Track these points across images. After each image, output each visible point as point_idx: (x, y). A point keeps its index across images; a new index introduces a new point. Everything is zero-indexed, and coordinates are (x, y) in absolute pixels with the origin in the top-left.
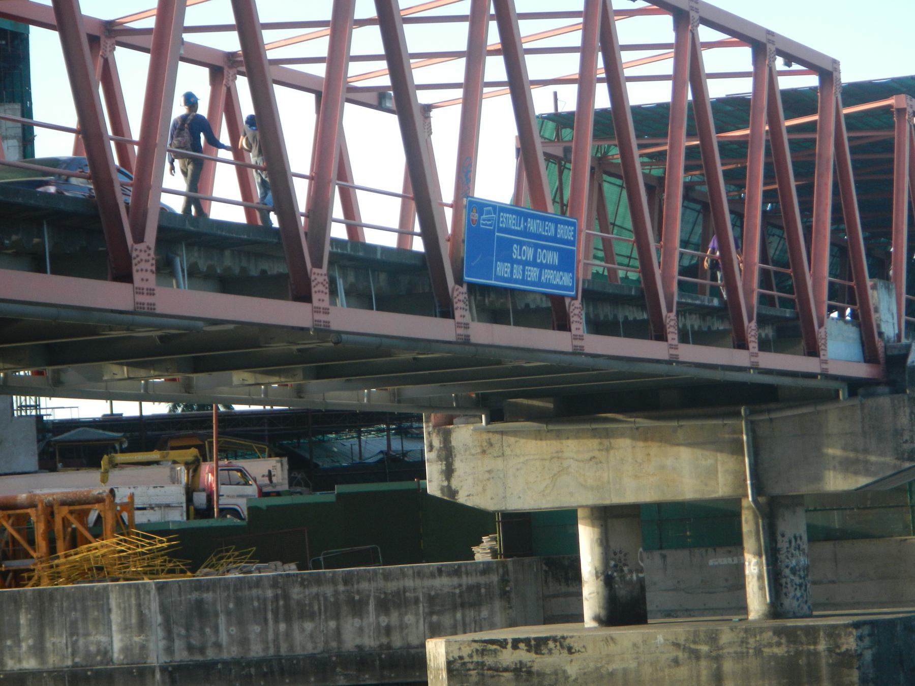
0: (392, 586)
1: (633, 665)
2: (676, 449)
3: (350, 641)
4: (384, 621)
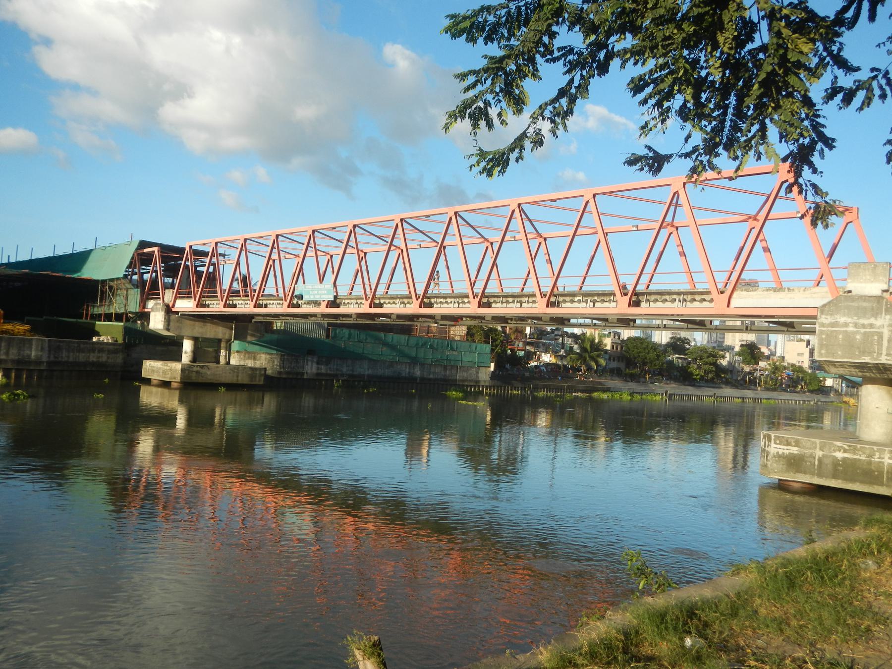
0: (101, 347)
1: (221, 372)
4: (99, 355)
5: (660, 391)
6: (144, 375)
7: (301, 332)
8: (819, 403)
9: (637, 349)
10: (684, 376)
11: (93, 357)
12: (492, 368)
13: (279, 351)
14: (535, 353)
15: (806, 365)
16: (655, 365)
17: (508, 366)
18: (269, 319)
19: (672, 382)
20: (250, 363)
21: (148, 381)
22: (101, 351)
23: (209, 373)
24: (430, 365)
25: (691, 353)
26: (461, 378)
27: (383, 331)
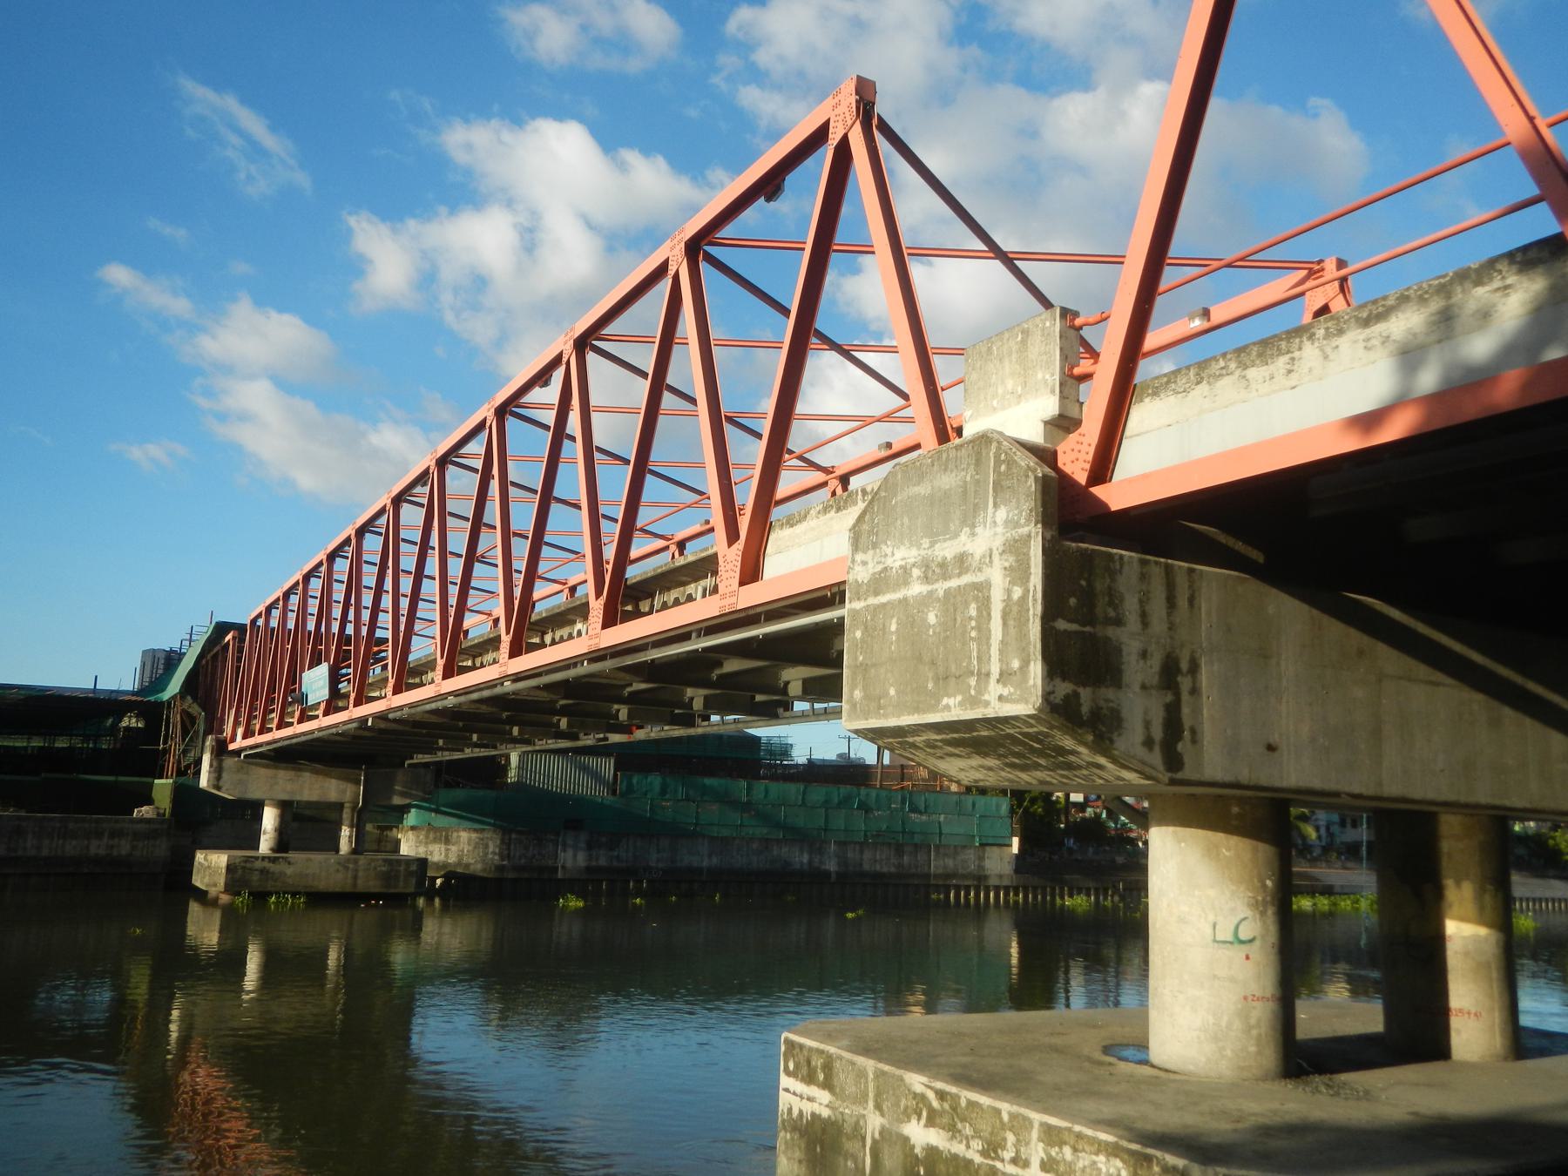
2: (328, 780)
3: (93, 850)
11: (97, 848)
12: (1015, 849)
24: (861, 844)
26: (940, 871)
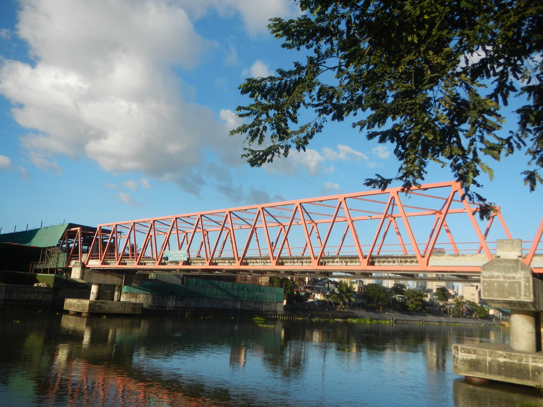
5: (390, 318)
6: (65, 308)
7: (166, 280)
8: (487, 325)
9: (374, 291)
10: (403, 308)
11: (33, 297)
12: (285, 303)
13: (152, 292)
14: (311, 294)
15: (477, 301)
16: (385, 302)
17: (295, 302)
18: (148, 272)
19: (396, 312)
20: (133, 300)
21: (67, 312)
22: (39, 292)
23: (106, 306)
25: (407, 293)
26: (266, 310)
27: (218, 280)
